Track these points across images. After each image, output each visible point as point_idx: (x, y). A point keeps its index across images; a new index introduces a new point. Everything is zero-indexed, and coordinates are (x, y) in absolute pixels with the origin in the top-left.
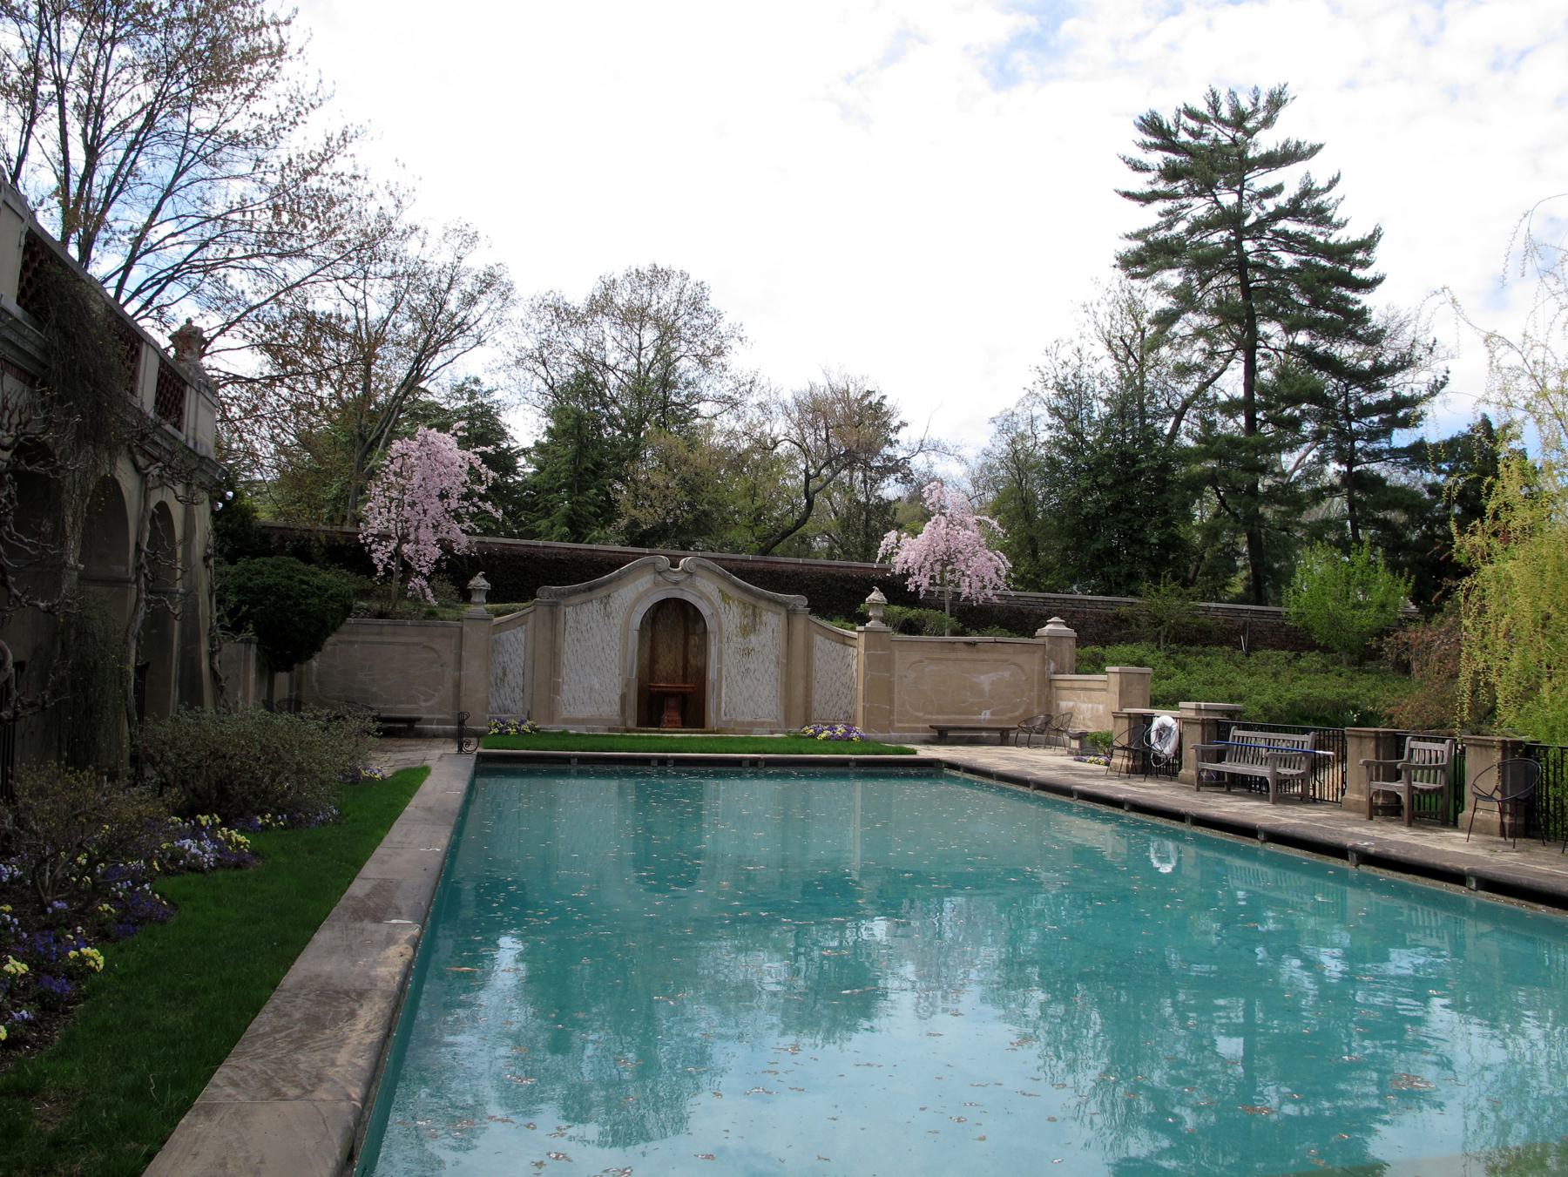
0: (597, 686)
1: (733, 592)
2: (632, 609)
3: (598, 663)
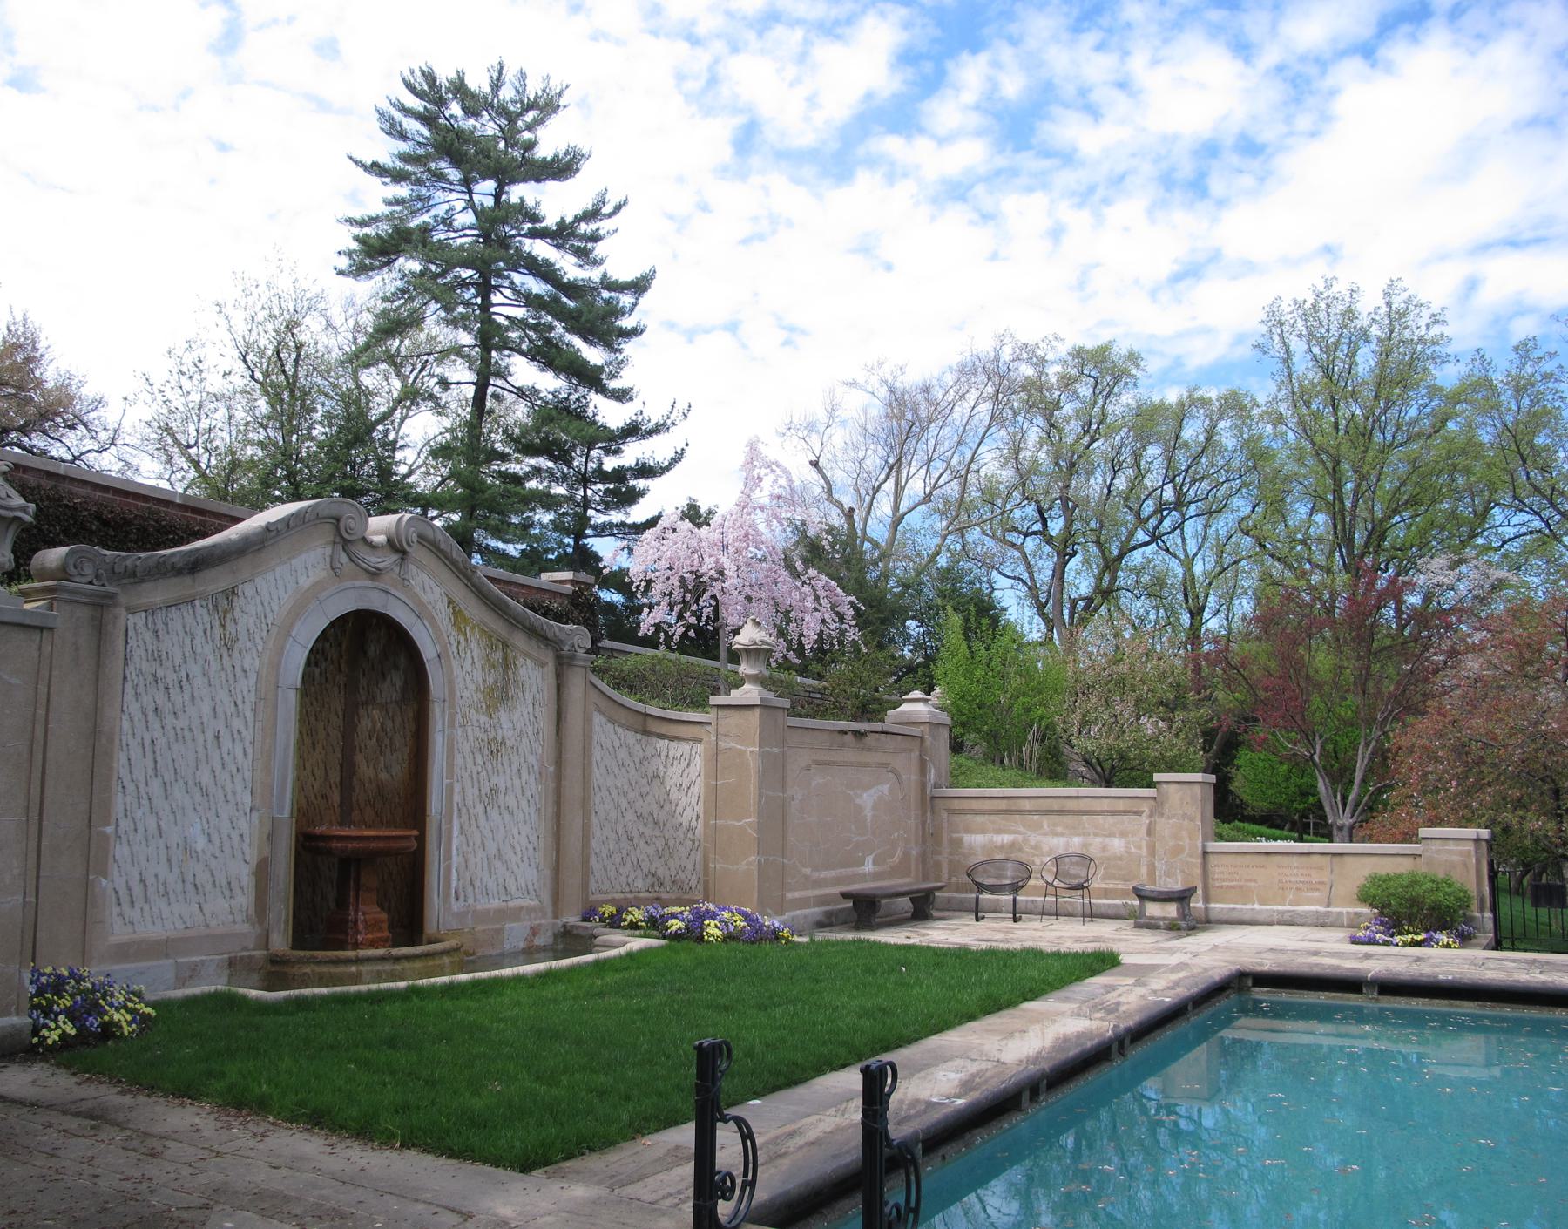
0: (200, 844)
3: (206, 779)
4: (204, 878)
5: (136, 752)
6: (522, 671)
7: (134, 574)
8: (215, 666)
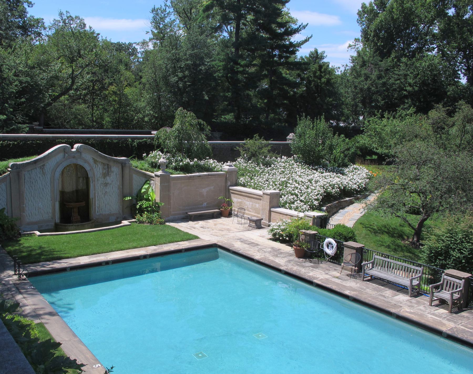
1: (98, 159)
6: (113, 169)
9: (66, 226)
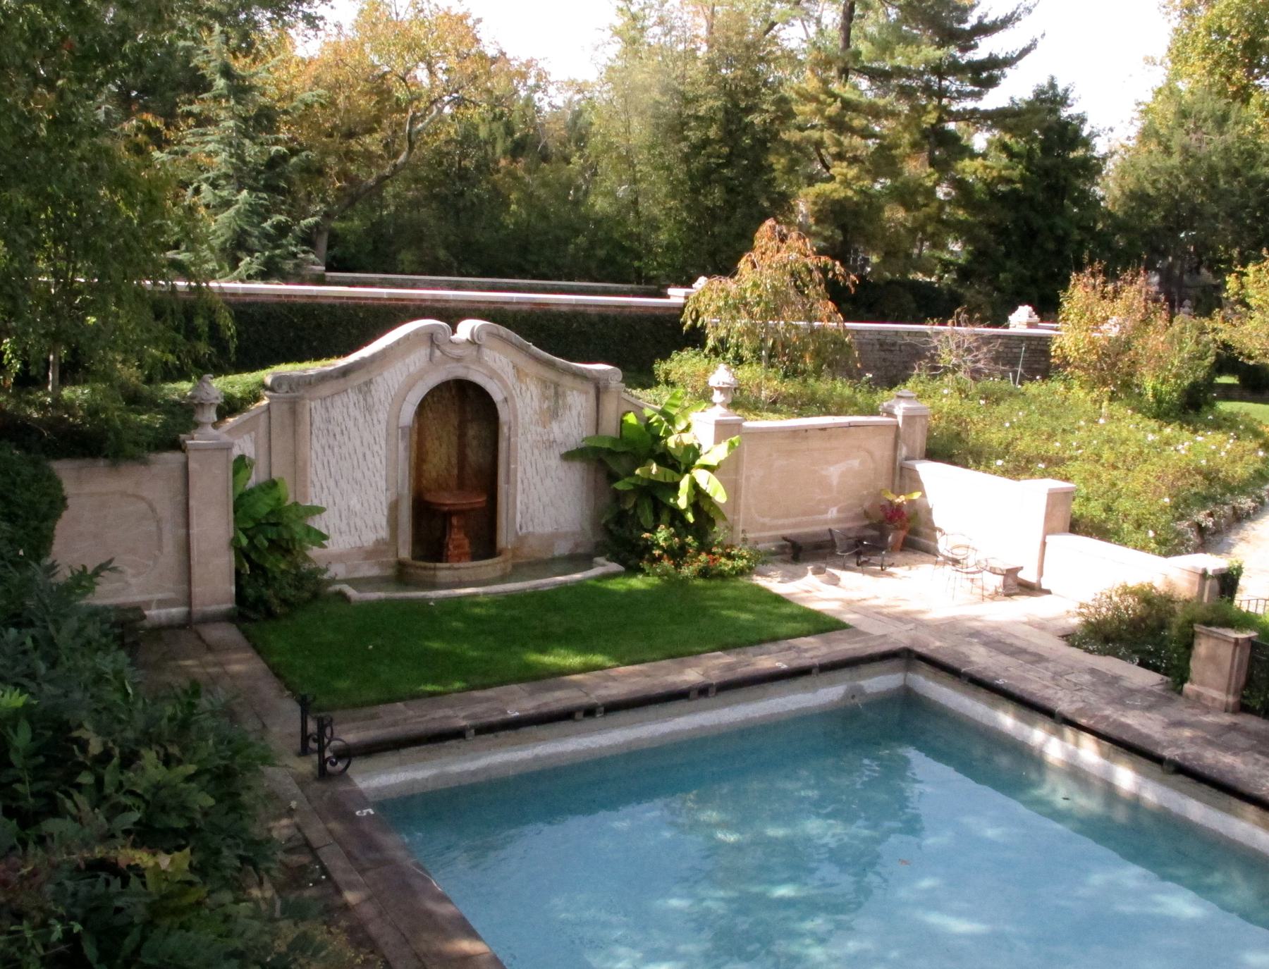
1: (532, 368)
2: (401, 398)
3: (359, 475)
4: (359, 523)
5: (319, 466)
7: (310, 384)
8: (361, 420)
9: (435, 569)
